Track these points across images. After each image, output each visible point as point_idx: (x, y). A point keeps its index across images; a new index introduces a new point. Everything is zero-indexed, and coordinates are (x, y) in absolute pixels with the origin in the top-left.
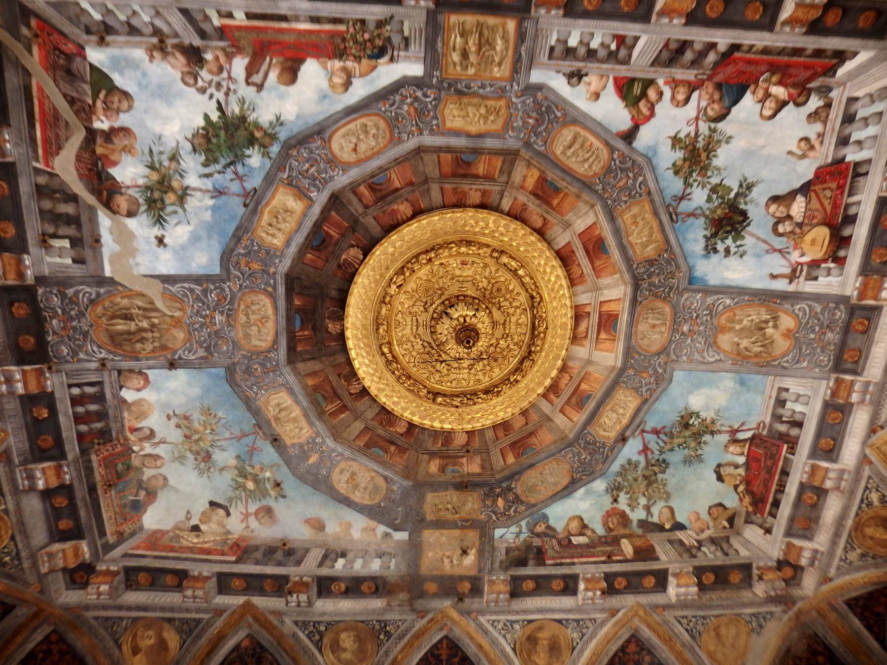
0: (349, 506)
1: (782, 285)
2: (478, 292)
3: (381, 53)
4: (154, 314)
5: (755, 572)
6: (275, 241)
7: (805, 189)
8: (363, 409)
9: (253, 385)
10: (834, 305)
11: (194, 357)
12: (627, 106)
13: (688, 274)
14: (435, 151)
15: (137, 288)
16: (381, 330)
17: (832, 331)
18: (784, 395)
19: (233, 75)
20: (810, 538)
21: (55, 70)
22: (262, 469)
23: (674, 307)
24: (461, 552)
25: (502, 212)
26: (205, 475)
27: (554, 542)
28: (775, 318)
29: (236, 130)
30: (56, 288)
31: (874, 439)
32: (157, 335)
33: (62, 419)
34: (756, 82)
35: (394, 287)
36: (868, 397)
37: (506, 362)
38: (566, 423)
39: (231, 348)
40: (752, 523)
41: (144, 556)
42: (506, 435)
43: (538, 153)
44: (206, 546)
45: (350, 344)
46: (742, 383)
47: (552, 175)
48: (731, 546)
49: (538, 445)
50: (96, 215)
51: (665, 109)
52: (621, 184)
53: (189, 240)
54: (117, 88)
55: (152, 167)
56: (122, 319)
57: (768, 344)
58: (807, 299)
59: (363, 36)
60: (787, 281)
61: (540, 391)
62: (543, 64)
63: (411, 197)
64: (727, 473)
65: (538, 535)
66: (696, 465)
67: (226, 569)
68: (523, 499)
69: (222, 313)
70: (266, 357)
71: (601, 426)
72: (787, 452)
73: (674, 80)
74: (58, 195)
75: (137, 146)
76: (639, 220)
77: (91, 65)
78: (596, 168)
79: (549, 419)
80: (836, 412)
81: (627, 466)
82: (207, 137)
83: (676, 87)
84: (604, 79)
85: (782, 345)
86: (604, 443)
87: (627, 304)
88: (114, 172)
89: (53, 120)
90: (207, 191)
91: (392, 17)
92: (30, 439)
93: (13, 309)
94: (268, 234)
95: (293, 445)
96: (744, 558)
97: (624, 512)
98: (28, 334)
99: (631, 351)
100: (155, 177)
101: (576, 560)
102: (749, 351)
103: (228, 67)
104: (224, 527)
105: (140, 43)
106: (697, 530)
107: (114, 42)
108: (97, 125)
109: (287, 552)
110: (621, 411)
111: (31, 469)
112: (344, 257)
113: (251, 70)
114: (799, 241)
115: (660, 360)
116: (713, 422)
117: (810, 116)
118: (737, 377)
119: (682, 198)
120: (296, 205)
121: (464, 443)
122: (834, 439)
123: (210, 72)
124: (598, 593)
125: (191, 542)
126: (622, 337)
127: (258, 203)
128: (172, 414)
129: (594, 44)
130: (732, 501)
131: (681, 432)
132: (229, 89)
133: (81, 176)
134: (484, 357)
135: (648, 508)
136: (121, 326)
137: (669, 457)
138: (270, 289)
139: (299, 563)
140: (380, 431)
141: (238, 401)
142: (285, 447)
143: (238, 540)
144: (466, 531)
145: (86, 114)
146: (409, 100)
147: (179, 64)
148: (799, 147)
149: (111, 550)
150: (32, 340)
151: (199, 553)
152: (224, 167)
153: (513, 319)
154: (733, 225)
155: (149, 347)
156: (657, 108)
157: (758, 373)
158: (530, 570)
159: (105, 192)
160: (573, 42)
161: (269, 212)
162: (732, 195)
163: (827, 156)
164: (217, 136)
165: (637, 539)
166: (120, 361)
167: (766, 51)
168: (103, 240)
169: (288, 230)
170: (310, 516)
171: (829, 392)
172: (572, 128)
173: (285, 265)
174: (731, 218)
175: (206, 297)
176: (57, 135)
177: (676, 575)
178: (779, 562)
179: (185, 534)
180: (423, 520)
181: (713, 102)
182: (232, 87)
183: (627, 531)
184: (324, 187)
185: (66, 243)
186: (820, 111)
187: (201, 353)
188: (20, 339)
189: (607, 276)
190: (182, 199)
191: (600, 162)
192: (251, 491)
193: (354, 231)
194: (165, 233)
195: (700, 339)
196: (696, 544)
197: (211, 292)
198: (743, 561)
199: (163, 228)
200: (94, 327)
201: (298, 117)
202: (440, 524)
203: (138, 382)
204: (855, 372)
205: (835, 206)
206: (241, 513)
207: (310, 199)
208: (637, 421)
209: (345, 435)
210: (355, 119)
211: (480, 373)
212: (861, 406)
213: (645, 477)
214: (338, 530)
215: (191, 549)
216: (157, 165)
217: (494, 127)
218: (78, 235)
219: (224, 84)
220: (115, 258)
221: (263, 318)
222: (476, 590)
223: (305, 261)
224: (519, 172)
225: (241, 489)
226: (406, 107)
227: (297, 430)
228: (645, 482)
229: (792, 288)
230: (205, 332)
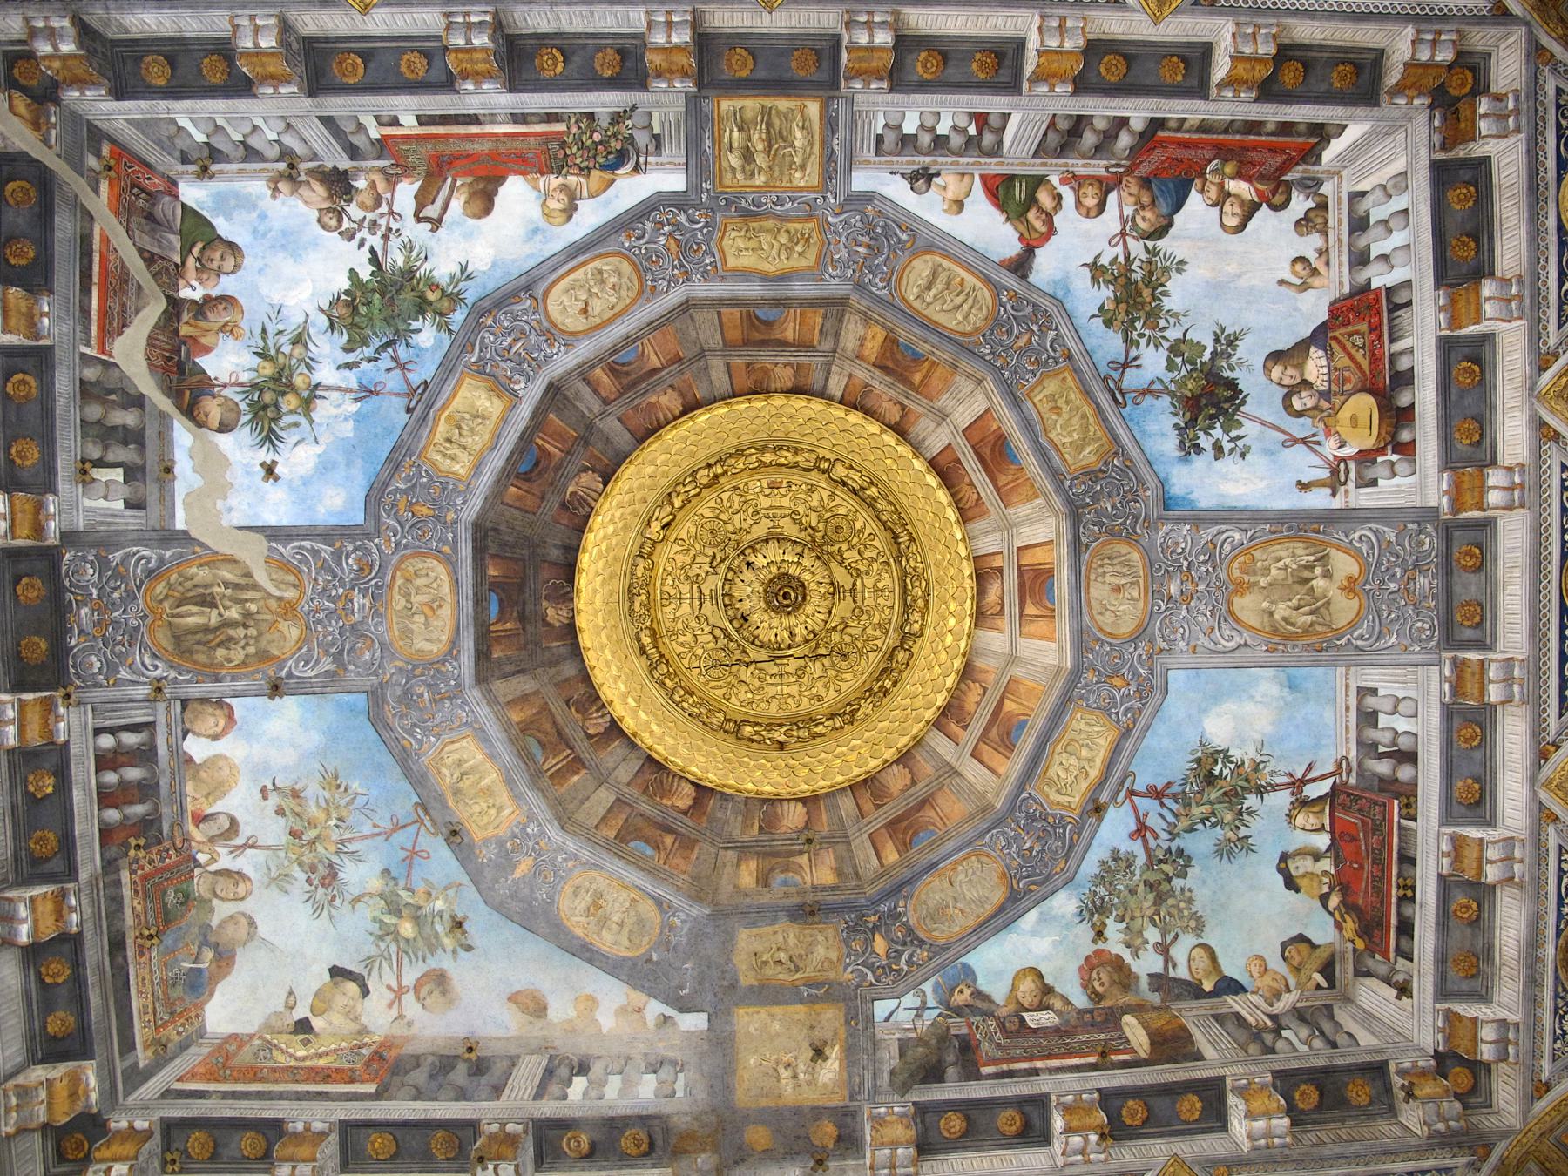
0: (590, 962)
1: (1319, 499)
2: (803, 535)
3: (620, 159)
5: (1397, 1081)
6: (456, 467)
7: (1320, 336)
8: (611, 765)
9: (414, 725)
10: (1415, 526)
11: (313, 674)
12: (1008, 219)
13: (1160, 493)
14: (712, 306)
15: (225, 549)
16: (637, 604)
17: (1424, 572)
18: (1370, 701)
20: (1484, 997)
22: (429, 894)
23: (1146, 552)
24: (811, 1053)
25: (831, 399)
26: (325, 912)
27: (992, 1025)
28: (1323, 559)
29: (398, 293)
30: (93, 551)
31: (1547, 771)
32: (252, 632)
33: (77, 795)
34: (1202, 175)
35: (656, 526)
36: (1516, 688)
37: (863, 662)
38: (987, 778)
39: (378, 655)
40: (1369, 974)
41: (201, 1095)
42: (878, 807)
43: (880, 300)
44: (321, 1062)
45: (585, 640)
46: (1292, 686)
47: (903, 335)
48: (1338, 1026)
49: (940, 824)
51: (1067, 219)
52: (1021, 343)
53: (316, 468)
54: (220, 237)
55: (263, 355)
56: (196, 604)
57: (1319, 607)
58: (1368, 520)
60: (1329, 491)
61: (929, 714)
62: (869, 162)
63: (677, 381)
64: (1301, 871)
65: (958, 1011)
66: (1241, 859)
67: (357, 1111)
68: (922, 935)
69: (364, 592)
70: (438, 670)
71: (1051, 783)
72: (1401, 816)
73: (1074, 176)
74: (113, 397)
75: (244, 324)
76: (1060, 403)
77: (184, 205)
78: (977, 319)
79: (956, 773)
80: (1469, 724)
81: (1112, 864)
82: (352, 306)
83: (1080, 186)
84: (967, 178)
85: (1345, 608)
86: (1062, 817)
87: (1064, 550)
88: (208, 363)
90: (351, 390)
91: (634, 108)
92: (15, 838)
93: (19, 589)
94: (444, 455)
95: (486, 841)
96: (1369, 1051)
97: (1118, 956)
98: (37, 633)
99: (1085, 637)
100: (268, 369)
101: (1039, 1064)
102: (1293, 625)
103: (389, 196)
104: (356, 1019)
105: (261, 170)
106: (1268, 995)
107: (222, 172)
108: (185, 293)
109: (473, 1065)
110: (1084, 753)
111: (10, 900)
112: (571, 489)
113: (422, 200)
114: (1330, 421)
115: (1139, 651)
116: (1256, 767)
117: (1298, 223)
118: (1283, 676)
119: (1126, 365)
120: (491, 406)
121: (802, 825)
122: (1477, 780)
123: (362, 206)
124: (1093, 1138)
125: (291, 1056)
126: (1066, 611)
128: (270, 787)
129: (943, 128)
130: (1322, 931)
131: (1201, 792)
134: (823, 651)
135: (1164, 949)
136: (194, 617)
137: (1187, 842)
138: (446, 549)
139: (497, 1090)
140: (645, 807)
141: (387, 759)
142: (471, 846)
143: (382, 1045)
144: (817, 1007)
146: (667, 229)
147: (314, 198)
148: (1294, 273)
149: (141, 1085)
150: (43, 646)
151: (306, 1081)
152: (377, 351)
153: (869, 582)
154: (1217, 405)
155: (238, 655)
156: (1058, 220)
157: (1317, 664)
158: (948, 1091)
160: (910, 127)
161: (448, 419)
162: (1207, 356)
163: (1341, 283)
164: (369, 303)
165: (1154, 1015)
166: (188, 682)
167: (1204, 127)
168: (176, 470)
169: (478, 448)
170: (517, 987)
171: (1446, 687)
172: (928, 257)
173: (472, 508)
174: (1212, 393)
175: (339, 564)
176: (124, 305)
177: (1242, 1092)
178: (1437, 1055)
179: (282, 1040)
180: (733, 986)
181: (1143, 208)
182: (394, 226)
183: (1131, 999)
185: (117, 475)
186: (1312, 215)
187: (327, 664)
188: (23, 643)
189: (1022, 502)
190: (307, 404)
191: (981, 309)
192: (407, 941)
193: (587, 443)
194: (277, 458)
195: (1202, 608)
196: (1269, 1023)
197: (347, 557)
198: (1367, 1059)
200: (149, 620)
201: (494, 265)
202: (767, 994)
203: (212, 720)
204: (1481, 645)
205: (1375, 360)
206: (389, 987)
207: (514, 394)
208: (1117, 773)
209: (580, 816)
210: (584, 264)
211: (819, 684)
212: (1508, 708)
213: (1150, 886)
214: (572, 1013)
215: (291, 1073)
216: (273, 352)
217: (804, 263)
218: (139, 461)
219: (383, 222)
220: (193, 498)
221: (434, 601)
222: (849, 1142)
223: (507, 500)
224: (852, 331)
225: (388, 939)
227: (493, 812)
228: (1151, 897)
229: (1338, 503)
230: (334, 626)
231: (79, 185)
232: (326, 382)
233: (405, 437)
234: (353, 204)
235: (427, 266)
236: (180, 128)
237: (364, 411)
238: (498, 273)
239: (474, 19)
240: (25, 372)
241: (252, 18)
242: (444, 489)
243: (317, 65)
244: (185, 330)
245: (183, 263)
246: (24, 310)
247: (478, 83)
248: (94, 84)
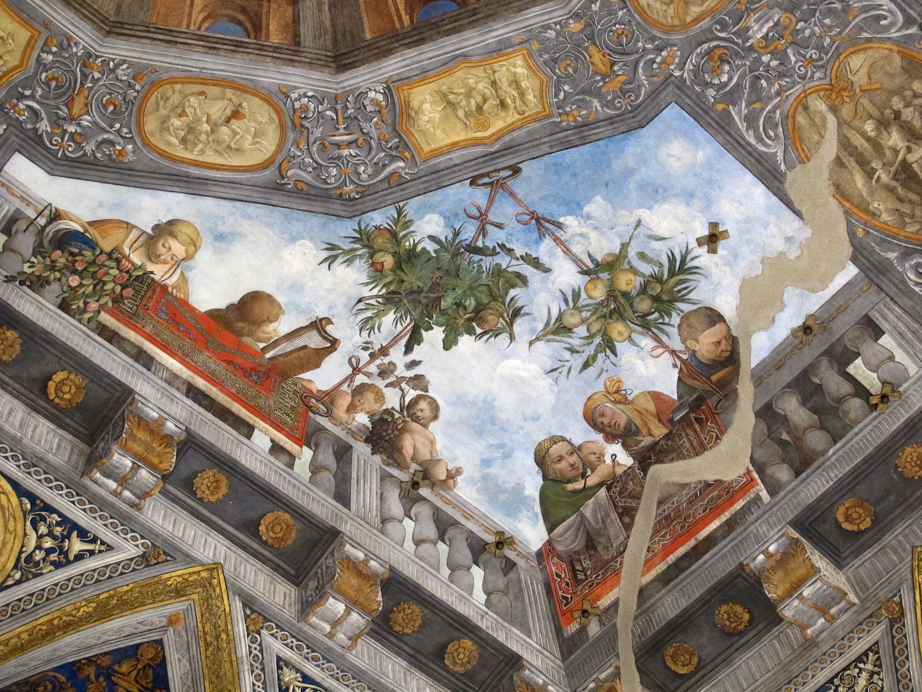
3: (65, 240)
4: (858, 141)
6: (521, 70)
15: (834, 208)
19: (349, 371)
21: (608, 562)
29: (420, 291)
50: (763, 364)
53: (664, 199)
55: (609, 345)
59: (81, 285)
69: (744, 33)
74: (785, 437)
75: (600, 387)
77: (550, 530)
89: (674, 521)
90: (557, 240)
91: (9, 279)
94: (522, 94)
100: (617, 329)
103: (344, 387)
105: (448, 502)
107: (487, 530)
108: (625, 460)
113: (315, 358)
120: (426, 104)
123: (380, 397)
127: (491, 156)
132: (373, 356)
133: (723, 429)
145: (626, 483)
146: (72, 129)
152: (494, 253)
159: (714, 378)
161: (485, 127)
169: (479, 71)
175: (737, 85)
176: (690, 502)
182: (365, 356)
184: (347, 94)
185: (857, 368)
190: (612, 264)
194: (693, 244)
197: (725, 85)
199: (688, 251)
201: (294, 239)
207: (388, 92)
216: (598, 340)
218: (825, 361)
219: (373, 368)
220: (810, 281)
226: (86, 121)
231: (625, 622)
232: (574, 268)
233: (545, 148)
234: (388, 405)
235: (366, 292)
236: (489, 594)
237: (563, 209)
238: (297, 227)
239: (113, 485)
240: (838, 525)
241: (330, 636)
242: (555, 61)
243: (308, 555)
244: (659, 431)
245: (600, 485)
246: (780, 573)
247: (160, 422)
248: (528, 684)
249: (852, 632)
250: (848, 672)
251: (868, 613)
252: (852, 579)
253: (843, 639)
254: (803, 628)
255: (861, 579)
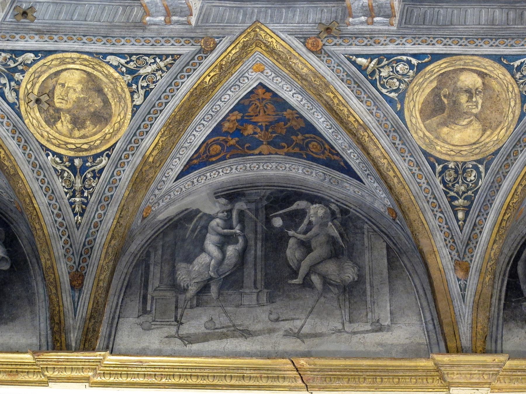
249: (172, 38)
250: (147, 58)
251: (193, 35)
252: (204, 10)
253: (163, 38)
254: (147, 13)
255: (209, 14)
